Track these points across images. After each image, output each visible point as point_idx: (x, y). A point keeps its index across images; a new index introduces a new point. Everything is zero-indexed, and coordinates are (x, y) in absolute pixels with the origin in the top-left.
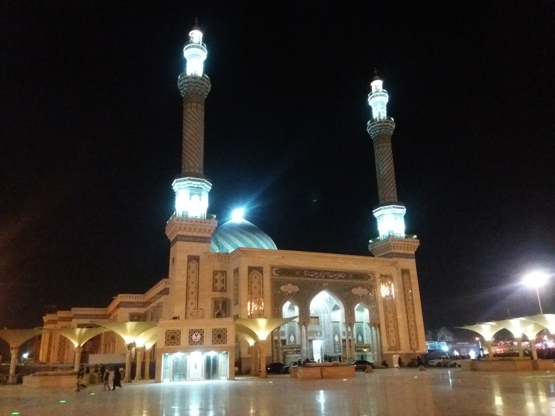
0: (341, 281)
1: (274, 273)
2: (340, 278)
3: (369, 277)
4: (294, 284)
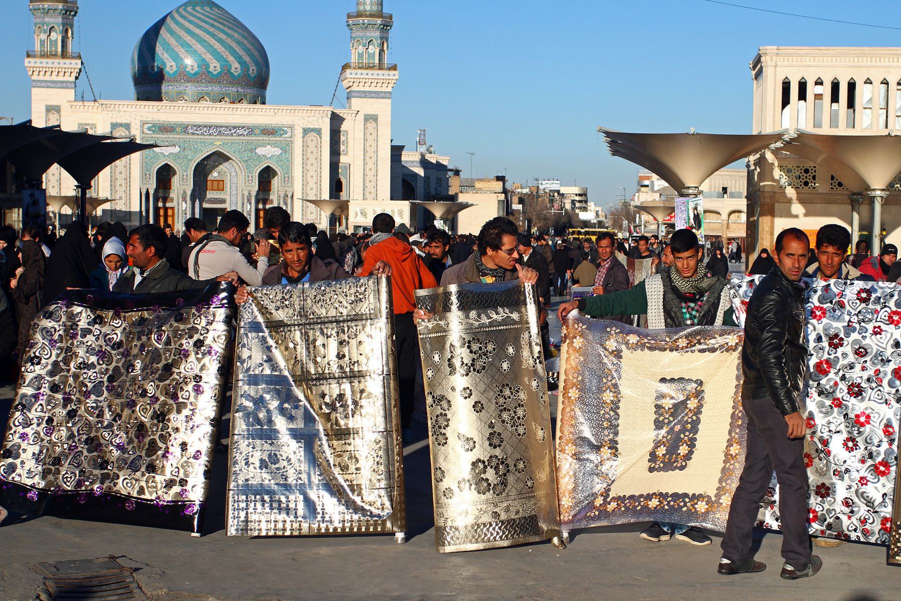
0: (241, 138)
1: (146, 131)
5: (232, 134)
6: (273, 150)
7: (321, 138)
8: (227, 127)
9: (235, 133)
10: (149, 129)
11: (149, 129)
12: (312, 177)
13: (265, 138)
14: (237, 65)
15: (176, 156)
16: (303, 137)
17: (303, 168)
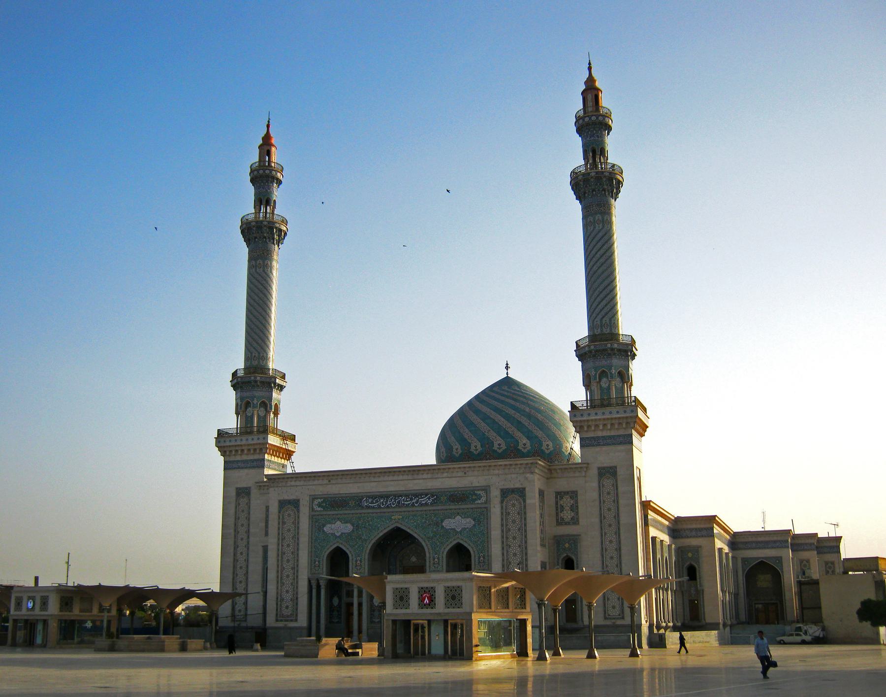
1: (316, 508)
2: (422, 505)
3: (480, 497)
5: (413, 505)
6: (464, 521)
7: (524, 501)
8: (406, 496)
9: (417, 502)
10: (319, 505)
11: (319, 505)
12: (515, 555)
13: (453, 507)
14: (525, 440)
15: (348, 537)
16: (502, 502)
17: (503, 543)
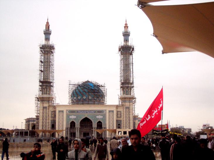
1: (68, 112)
3: (104, 112)
4: (74, 115)
8: (89, 111)
10: (68, 112)
11: (68, 112)
15: (75, 119)
